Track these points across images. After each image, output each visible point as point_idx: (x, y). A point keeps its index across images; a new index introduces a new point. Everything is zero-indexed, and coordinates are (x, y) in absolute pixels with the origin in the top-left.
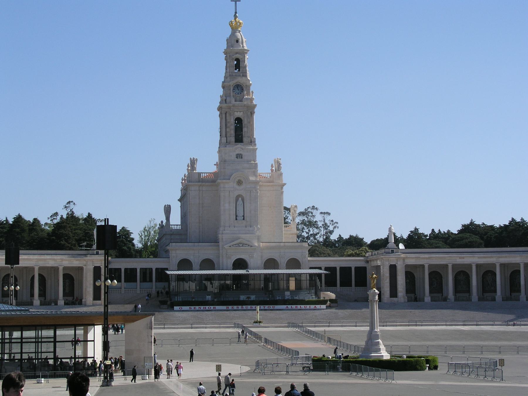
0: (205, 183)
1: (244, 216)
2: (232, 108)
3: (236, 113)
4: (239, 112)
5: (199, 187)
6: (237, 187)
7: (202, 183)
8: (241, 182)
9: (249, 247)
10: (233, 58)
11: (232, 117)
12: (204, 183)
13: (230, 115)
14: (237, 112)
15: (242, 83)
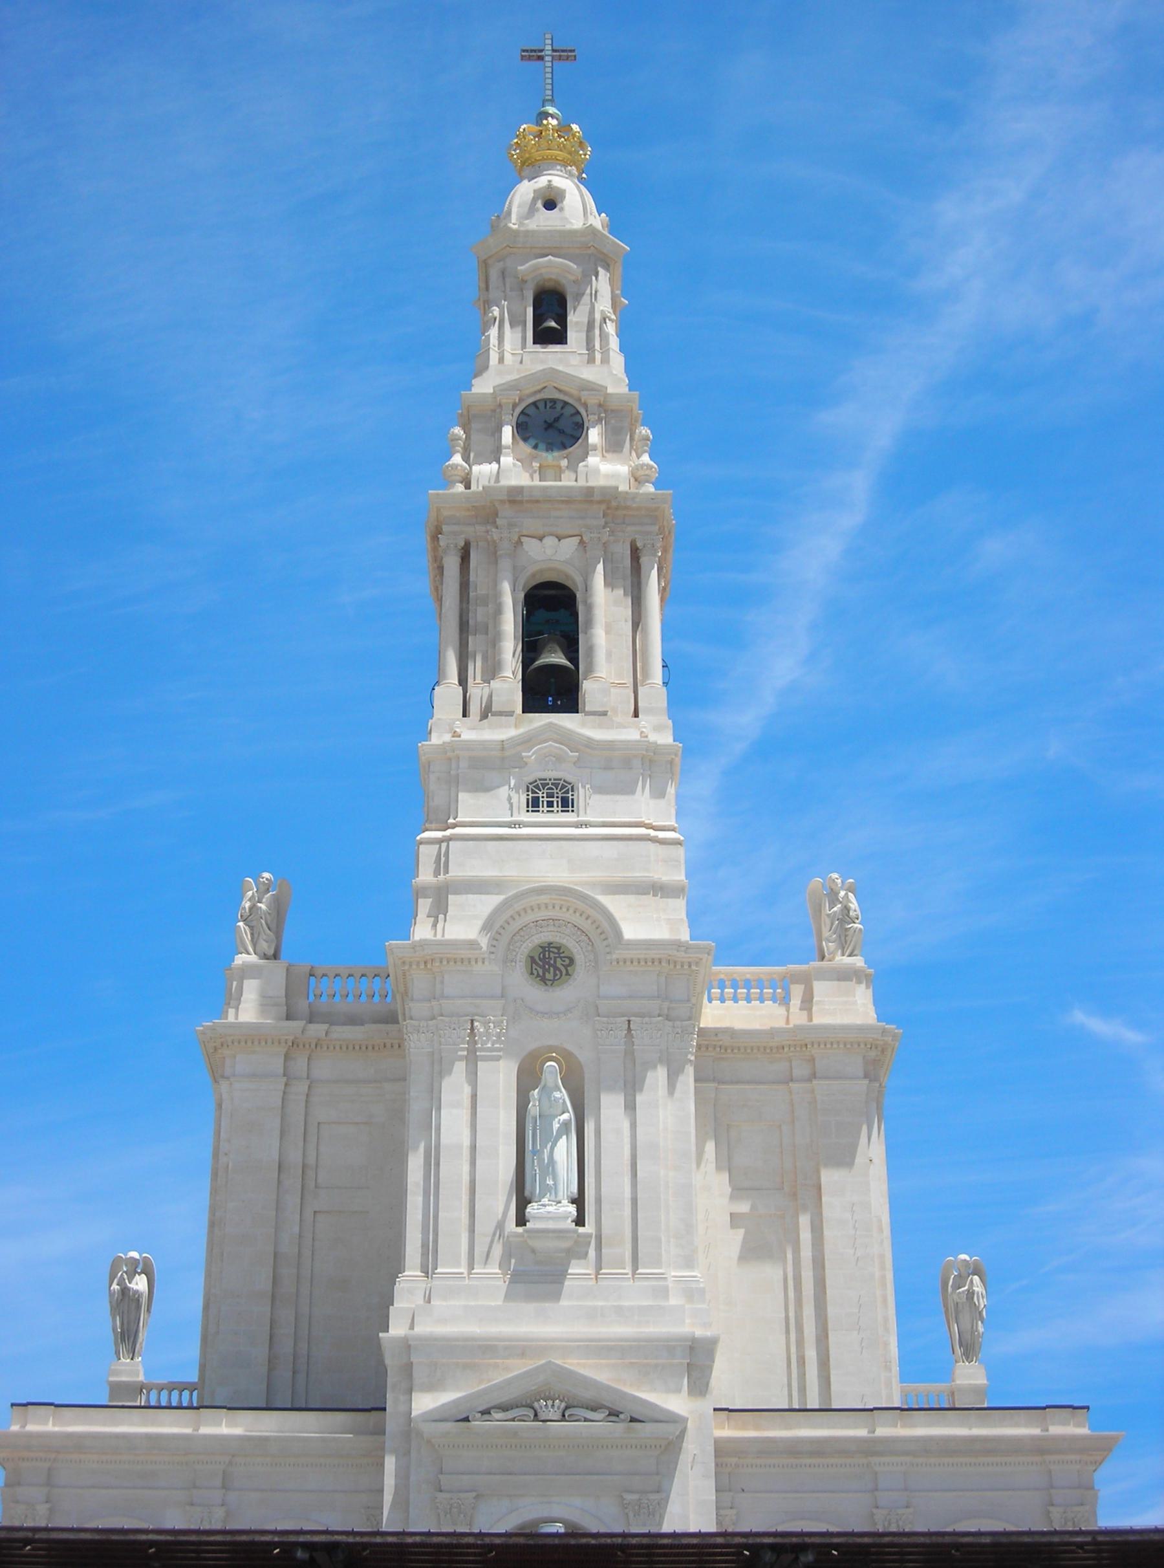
0: (325, 1026)
1: (579, 1201)
2: (506, 512)
3: (532, 547)
4: (550, 541)
5: (287, 1057)
6: (535, 993)
7: (312, 1026)
8: (558, 959)
9: (617, 1429)
10: (524, 282)
11: (505, 564)
12: (317, 1030)
13: (494, 556)
14: (541, 539)
15: (574, 392)
